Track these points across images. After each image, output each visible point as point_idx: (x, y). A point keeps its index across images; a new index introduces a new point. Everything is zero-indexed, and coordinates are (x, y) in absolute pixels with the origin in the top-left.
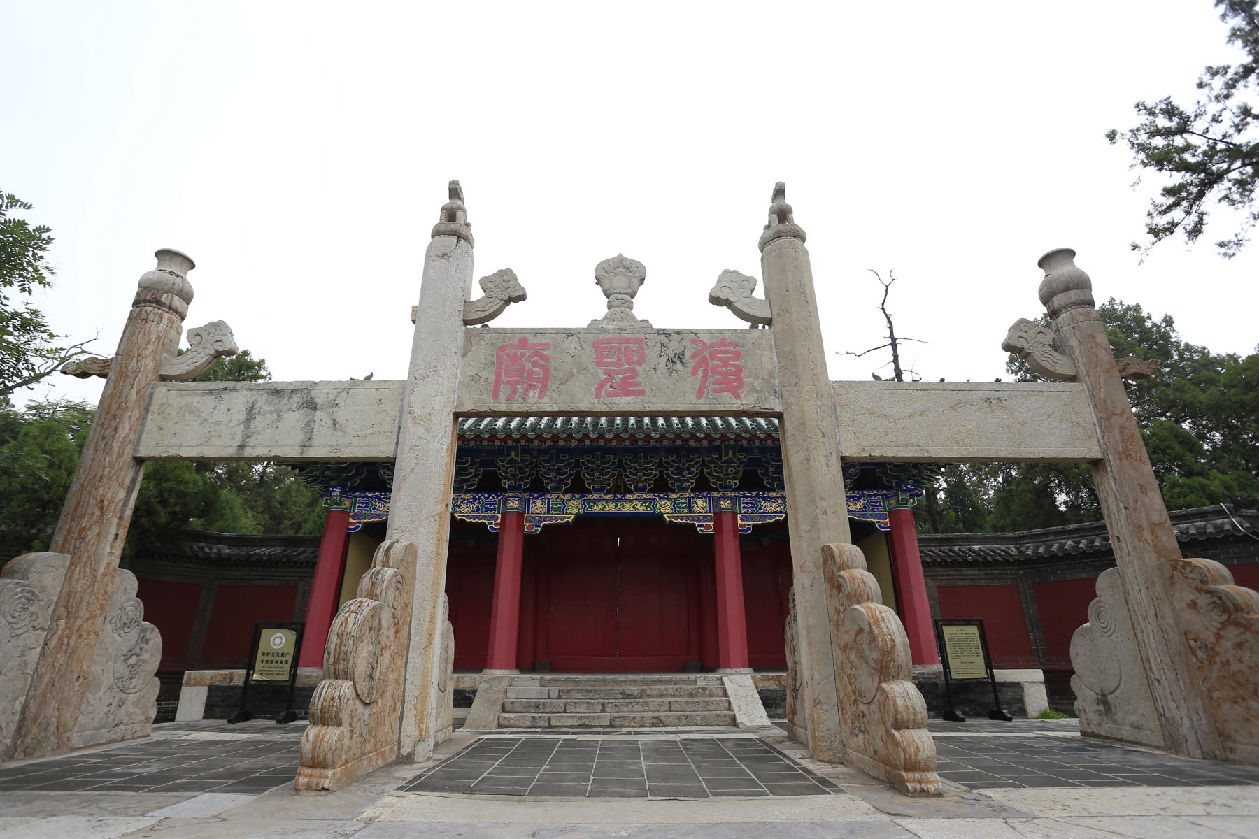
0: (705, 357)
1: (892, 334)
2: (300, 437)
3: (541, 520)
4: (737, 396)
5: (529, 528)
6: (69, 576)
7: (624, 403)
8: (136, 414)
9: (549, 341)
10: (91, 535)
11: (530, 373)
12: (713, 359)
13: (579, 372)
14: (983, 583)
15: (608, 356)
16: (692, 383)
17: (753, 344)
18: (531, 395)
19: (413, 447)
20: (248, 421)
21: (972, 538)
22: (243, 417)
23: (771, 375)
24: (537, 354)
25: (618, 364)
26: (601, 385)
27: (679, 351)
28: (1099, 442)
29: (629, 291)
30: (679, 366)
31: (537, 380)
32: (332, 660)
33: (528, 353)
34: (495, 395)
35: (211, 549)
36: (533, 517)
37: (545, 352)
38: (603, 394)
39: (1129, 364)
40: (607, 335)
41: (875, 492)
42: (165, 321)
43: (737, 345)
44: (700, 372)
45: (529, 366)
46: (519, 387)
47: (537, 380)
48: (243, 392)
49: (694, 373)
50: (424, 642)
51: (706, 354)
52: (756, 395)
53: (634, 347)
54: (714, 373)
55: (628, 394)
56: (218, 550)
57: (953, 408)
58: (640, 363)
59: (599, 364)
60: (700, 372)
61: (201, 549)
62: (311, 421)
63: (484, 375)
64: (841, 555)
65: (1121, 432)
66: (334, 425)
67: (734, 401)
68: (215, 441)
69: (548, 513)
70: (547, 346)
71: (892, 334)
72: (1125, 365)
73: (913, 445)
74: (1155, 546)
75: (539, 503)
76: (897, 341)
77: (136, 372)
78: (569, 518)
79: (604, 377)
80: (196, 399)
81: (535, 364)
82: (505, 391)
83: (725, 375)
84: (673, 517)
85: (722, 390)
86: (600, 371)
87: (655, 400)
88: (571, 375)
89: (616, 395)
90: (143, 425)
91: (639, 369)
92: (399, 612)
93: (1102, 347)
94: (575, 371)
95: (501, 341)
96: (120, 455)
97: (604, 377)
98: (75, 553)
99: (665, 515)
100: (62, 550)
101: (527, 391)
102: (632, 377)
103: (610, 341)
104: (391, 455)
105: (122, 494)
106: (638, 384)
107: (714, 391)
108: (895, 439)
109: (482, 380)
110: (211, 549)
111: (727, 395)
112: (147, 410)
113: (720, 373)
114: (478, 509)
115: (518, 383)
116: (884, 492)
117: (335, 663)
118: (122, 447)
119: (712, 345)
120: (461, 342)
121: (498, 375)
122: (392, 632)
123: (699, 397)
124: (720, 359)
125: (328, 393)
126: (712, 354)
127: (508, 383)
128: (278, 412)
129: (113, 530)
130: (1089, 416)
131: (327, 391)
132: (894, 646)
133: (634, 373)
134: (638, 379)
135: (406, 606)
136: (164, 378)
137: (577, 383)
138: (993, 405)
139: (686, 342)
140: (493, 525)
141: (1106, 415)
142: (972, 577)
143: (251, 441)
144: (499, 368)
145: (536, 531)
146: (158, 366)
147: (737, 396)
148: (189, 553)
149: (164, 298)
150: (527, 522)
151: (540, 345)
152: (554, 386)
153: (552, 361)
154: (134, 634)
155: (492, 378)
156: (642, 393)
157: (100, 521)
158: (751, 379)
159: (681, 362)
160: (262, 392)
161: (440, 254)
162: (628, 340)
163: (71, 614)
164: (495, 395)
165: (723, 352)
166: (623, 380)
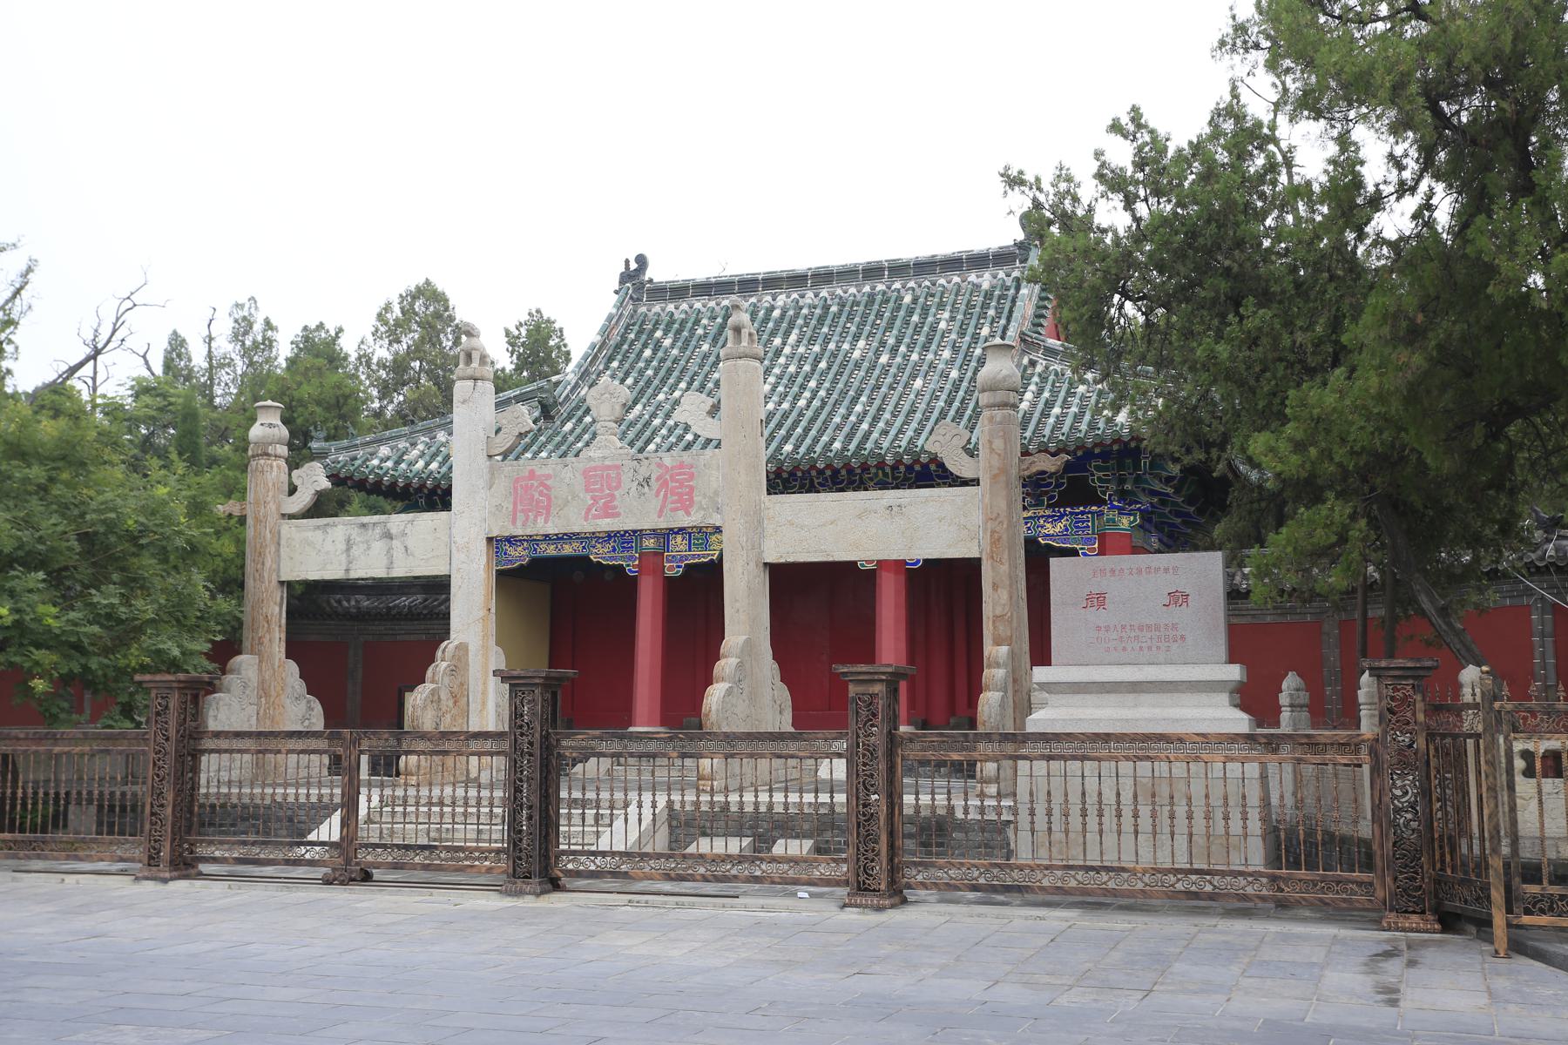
2: (385, 562)
3: (682, 559)
4: (688, 514)
5: (671, 568)
6: (260, 669)
8: (273, 549)
9: (551, 472)
10: (266, 640)
11: (538, 502)
13: (573, 498)
14: (1269, 619)
15: (595, 483)
16: (656, 503)
20: (348, 550)
22: (344, 547)
23: (716, 493)
25: (601, 490)
26: (589, 510)
34: (514, 522)
35: (348, 601)
39: (1034, 462)
40: (592, 464)
42: (275, 469)
45: (537, 496)
48: (340, 527)
49: (657, 495)
50: (479, 707)
53: (613, 474)
55: (607, 516)
56: (357, 601)
57: (859, 516)
58: (618, 487)
59: (587, 490)
61: (339, 602)
62: (390, 549)
63: (505, 505)
68: (328, 567)
70: (548, 477)
77: (265, 516)
79: (591, 502)
80: (310, 534)
81: (541, 494)
82: (520, 516)
83: (681, 495)
85: (676, 509)
87: (627, 521)
90: (279, 556)
92: (456, 689)
96: (270, 582)
97: (591, 502)
98: (259, 654)
101: (536, 517)
102: (611, 501)
103: (595, 469)
105: (277, 609)
106: (616, 507)
110: (348, 601)
111: (681, 513)
112: (279, 544)
114: (614, 550)
116: (1094, 508)
118: (270, 576)
121: (515, 504)
122: (451, 703)
123: (659, 517)
124: (677, 481)
126: (672, 476)
127: (522, 511)
128: (367, 542)
129: (277, 636)
130: (977, 518)
135: (462, 684)
136: (283, 515)
139: (653, 467)
140: (631, 567)
144: (515, 498)
146: (278, 508)
147: (688, 514)
148: (328, 609)
149: (270, 450)
150: (668, 561)
154: (303, 703)
155: (511, 507)
156: (618, 515)
157: (269, 631)
162: (609, 468)
163: (267, 695)
164: (514, 522)
165: (680, 474)
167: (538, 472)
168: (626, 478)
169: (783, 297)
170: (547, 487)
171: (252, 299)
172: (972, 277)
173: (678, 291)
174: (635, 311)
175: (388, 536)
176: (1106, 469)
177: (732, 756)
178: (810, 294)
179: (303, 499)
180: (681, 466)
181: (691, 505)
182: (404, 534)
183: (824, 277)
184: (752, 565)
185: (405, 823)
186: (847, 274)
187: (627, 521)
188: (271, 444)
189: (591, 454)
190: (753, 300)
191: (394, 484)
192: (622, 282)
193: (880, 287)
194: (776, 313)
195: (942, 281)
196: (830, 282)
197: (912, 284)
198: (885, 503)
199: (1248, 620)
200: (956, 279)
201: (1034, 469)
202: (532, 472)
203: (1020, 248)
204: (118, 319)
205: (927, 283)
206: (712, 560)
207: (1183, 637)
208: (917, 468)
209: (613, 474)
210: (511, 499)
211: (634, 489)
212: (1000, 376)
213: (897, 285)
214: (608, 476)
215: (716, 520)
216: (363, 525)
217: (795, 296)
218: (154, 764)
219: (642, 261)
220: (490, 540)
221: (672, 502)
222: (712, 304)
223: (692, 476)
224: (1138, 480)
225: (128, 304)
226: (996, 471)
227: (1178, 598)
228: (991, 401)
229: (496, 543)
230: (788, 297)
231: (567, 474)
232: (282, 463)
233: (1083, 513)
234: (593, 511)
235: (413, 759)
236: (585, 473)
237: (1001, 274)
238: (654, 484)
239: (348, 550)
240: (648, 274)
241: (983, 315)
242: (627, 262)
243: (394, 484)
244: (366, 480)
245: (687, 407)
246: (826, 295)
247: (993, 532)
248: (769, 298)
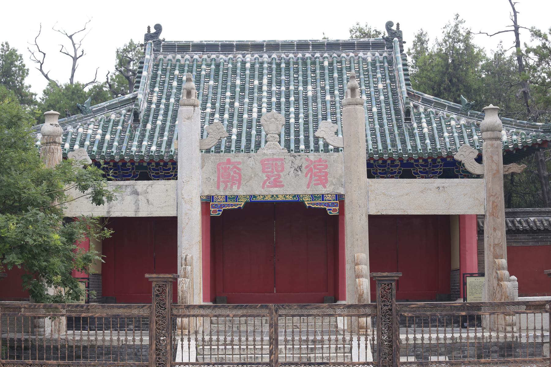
0: (312, 168)
1: (515, 22)
2: (134, 208)
3: (221, 206)
4: (325, 187)
7: (275, 191)
9: (241, 161)
11: (233, 177)
12: (315, 169)
13: (255, 176)
14: (530, 244)
15: (268, 168)
16: (305, 181)
17: (334, 161)
18: (234, 187)
19: (186, 214)
21: (531, 212)
23: (341, 176)
25: (272, 172)
26: (265, 183)
27: (300, 165)
28: (484, 207)
29: (277, 132)
30: (300, 172)
31: (236, 180)
32: (181, 299)
33: (231, 167)
34: (218, 187)
36: (216, 205)
37: (239, 166)
38: (266, 186)
39: (510, 168)
40: (267, 157)
43: (326, 162)
44: (309, 175)
45: (232, 173)
46: (228, 183)
47: (236, 180)
49: (306, 176)
51: (312, 166)
52: (333, 187)
53: (279, 163)
54: (315, 176)
55: (276, 186)
57: (422, 192)
58: (282, 171)
59: (263, 172)
60: (309, 175)
63: (212, 178)
64: (357, 260)
65: (492, 204)
66: (148, 202)
67: (324, 189)
69: (226, 201)
70: (239, 163)
71: (515, 22)
72: (509, 168)
73: (401, 209)
74: (493, 253)
76: (520, 29)
78: (240, 205)
79: (266, 178)
81: (235, 172)
82: (222, 186)
83: (320, 176)
84: (311, 203)
85: (318, 184)
86: (264, 175)
87: (288, 189)
88: (251, 178)
89: (271, 187)
91: (281, 174)
93: (495, 163)
94: (253, 175)
95: (218, 160)
97: (266, 178)
99: (306, 202)
101: (232, 186)
103: (268, 160)
104: (175, 215)
106: (281, 182)
107: (315, 184)
108: (393, 206)
109: (212, 180)
111: (320, 186)
113: (318, 176)
115: (228, 182)
117: (182, 300)
119: (315, 162)
120: (200, 162)
121: (219, 178)
123: (308, 188)
124: (318, 169)
125: (142, 187)
126: (314, 166)
127: (223, 182)
130: (483, 195)
131: (142, 186)
132: (363, 293)
133: (279, 176)
134: (281, 179)
137: (254, 182)
138: (440, 190)
139: (303, 160)
141: (490, 195)
142: (523, 241)
145: (219, 214)
147: (325, 187)
150: (213, 207)
151: (236, 162)
152: (244, 183)
153: (242, 171)
155: (216, 179)
156: (282, 186)
158: (332, 179)
159: (301, 171)
160: (112, 186)
161: (187, 118)
162: (276, 160)
164: (218, 187)
165: (320, 165)
166: (275, 180)
167: (233, 160)
168: (287, 166)
169: (249, 56)
170: (239, 169)
172: (361, 54)
173: (183, 48)
174: (156, 58)
175: (136, 193)
177: (494, 313)
178: (266, 56)
180: (320, 160)
181: (326, 182)
183: (273, 46)
184: (364, 215)
185: (233, 354)
186: (288, 46)
187: (288, 189)
188: (57, 136)
189: (265, 151)
190: (231, 56)
193: (308, 55)
194: (248, 65)
195: (344, 55)
196: (278, 50)
197: (326, 55)
198: (436, 185)
199: (521, 244)
200: (352, 54)
201: (510, 171)
203: (386, 41)
205: (335, 55)
206: (240, 208)
208: (380, 162)
209: (279, 163)
210: (216, 175)
211: (292, 172)
212: (496, 124)
213: (318, 55)
214: (276, 164)
217: (256, 56)
218: (156, 323)
219: (158, 28)
221: (315, 180)
222: (205, 56)
223: (326, 167)
226: (495, 172)
228: (492, 136)
230: (252, 56)
231: (251, 162)
234: (267, 183)
235: (186, 320)
236: (262, 162)
237: (377, 54)
238: (304, 170)
240: (161, 37)
241: (374, 76)
245: (322, 129)
246: (276, 57)
247: (493, 202)
248: (240, 56)
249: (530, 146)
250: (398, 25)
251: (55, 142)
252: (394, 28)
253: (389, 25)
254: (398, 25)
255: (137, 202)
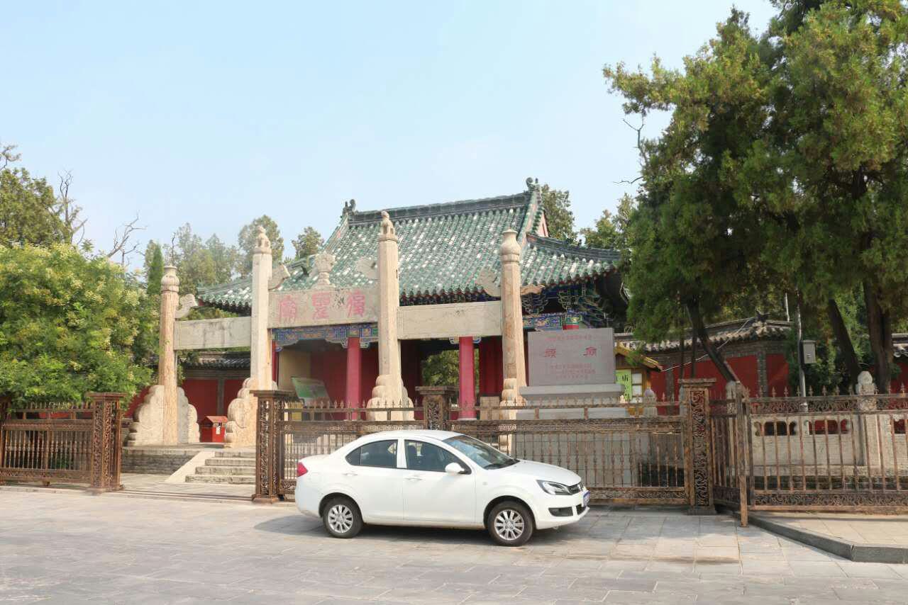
3: (370, 339)
4: (362, 316)
6: (165, 391)
10: (167, 378)
16: (346, 311)
20: (205, 334)
24: (293, 302)
26: (315, 315)
34: (280, 321)
41: (555, 314)
48: (201, 324)
55: (324, 317)
59: (314, 305)
75: (367, 330)
80: (188, 328)
100: (161, 384)
111: (358, 316)
121: (281, 314)
122: (250, 408)
123: (348, 317)
140: (345, 345)
143: (207, 342)
155: (279, 313)
164: (280, 321)
171: (188, 224)
175: (223, 328)
176: (566, 295)
179: (185, 311)
182: (230, 328)
191: (234, 306)
192: (344, 213)
202: (289, 297)
204: (125, 235)
207: (593, 371)
215: (375, 319)
216: (211, 323)
220: (269, 330)
224: (581, 300)
225: (130, 228)
227: (591, 351)
229: (272, 331)
231: (305, 298)
232: (176, 294)
233: (555, 316)
234: (317, 315)
236: (314, 298)
239: (205, 334)
242: (346, 203)
243: (234, 306)
244: (221, 304)
249: (608, 271)
250: (537, 180)
251: (168, 290)
252: (534, 183)
253: (529, 181)
254: (537, 180)
255: (223, 336)
